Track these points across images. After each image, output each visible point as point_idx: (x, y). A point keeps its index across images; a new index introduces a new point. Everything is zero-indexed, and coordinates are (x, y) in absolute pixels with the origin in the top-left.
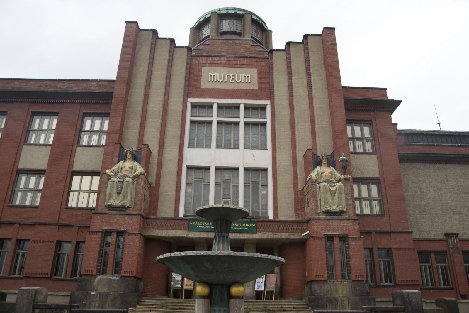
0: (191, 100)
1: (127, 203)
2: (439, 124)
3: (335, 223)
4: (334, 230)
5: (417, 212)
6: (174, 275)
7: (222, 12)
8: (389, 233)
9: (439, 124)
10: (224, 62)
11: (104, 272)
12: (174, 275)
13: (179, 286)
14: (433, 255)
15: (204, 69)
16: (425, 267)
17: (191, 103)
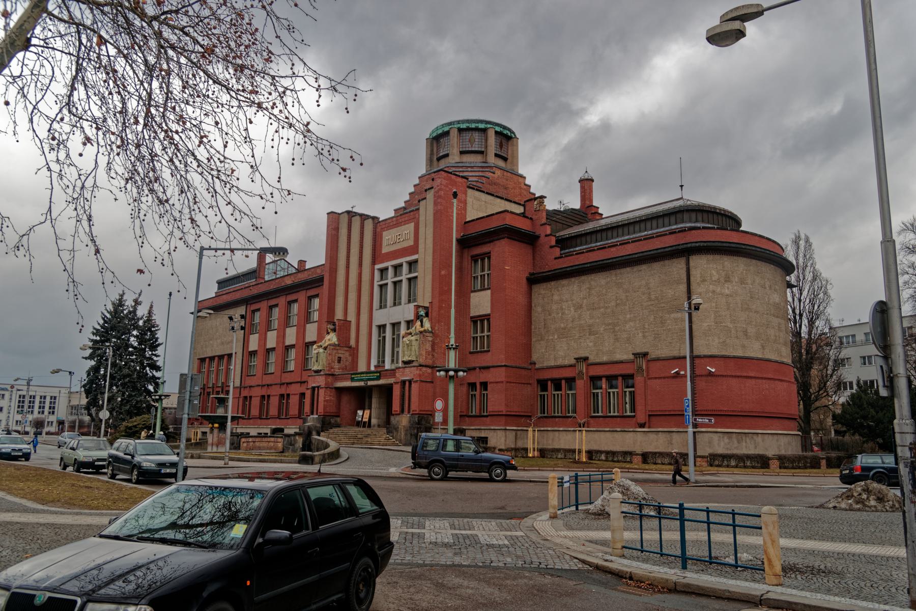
0: (377, 267)
1: (320, 368)
2: (682, 186)
3: (407, 370)
4: (406, 376)
5: (556, 337)
6: (359, 412)
7: (435, 135)
8: (488, 368)
9: (682, 186)
10: (395, 223)
11: (312, 414)
12: (359, 412)
13: (360, 419)
14: (563, 382)
15: (384, 233)
16: (558, 395)
17: (378, 269)
